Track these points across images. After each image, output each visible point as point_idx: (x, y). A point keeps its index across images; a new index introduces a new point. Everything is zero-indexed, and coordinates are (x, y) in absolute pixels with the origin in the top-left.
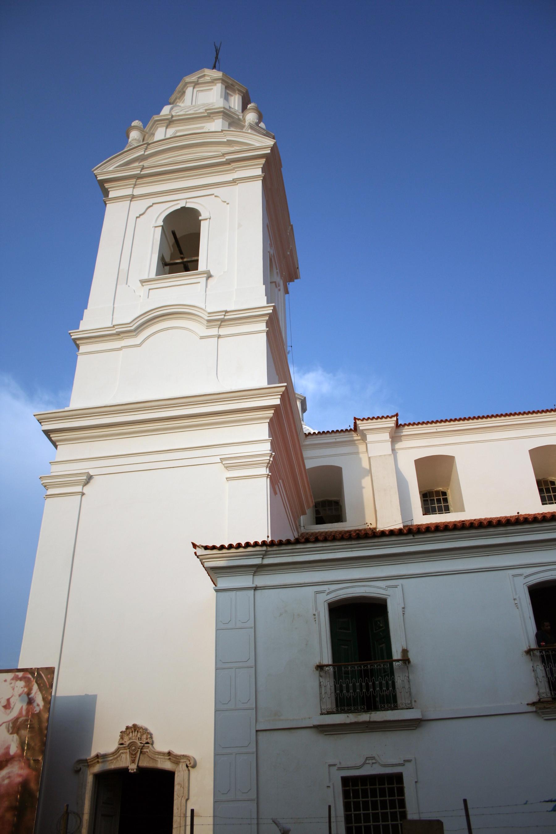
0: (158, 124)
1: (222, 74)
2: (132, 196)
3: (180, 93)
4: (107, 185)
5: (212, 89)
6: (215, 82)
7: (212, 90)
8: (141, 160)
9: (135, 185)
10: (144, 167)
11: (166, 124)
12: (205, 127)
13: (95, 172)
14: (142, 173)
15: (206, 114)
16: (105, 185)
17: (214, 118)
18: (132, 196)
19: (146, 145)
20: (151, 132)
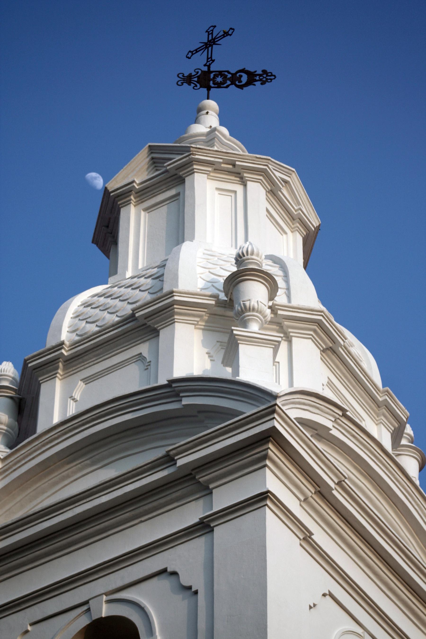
0: (315, 331)
1: (318, 224)
2: (308, 535)
3: (231, 166)
5: (286, 233)
6: (298, 225)
7: (285, 236)
8: (317, 434)
9: (306, 500)
10: (343, 483)
11: (324, 347)
12: (363, 422)
13: (278, 402)
14: (334, 492)
15: (380, 399)
16: (270, 446)
17: (383, 418)
18: (308, 535)
19: (341, 413)
20: (286, 323)
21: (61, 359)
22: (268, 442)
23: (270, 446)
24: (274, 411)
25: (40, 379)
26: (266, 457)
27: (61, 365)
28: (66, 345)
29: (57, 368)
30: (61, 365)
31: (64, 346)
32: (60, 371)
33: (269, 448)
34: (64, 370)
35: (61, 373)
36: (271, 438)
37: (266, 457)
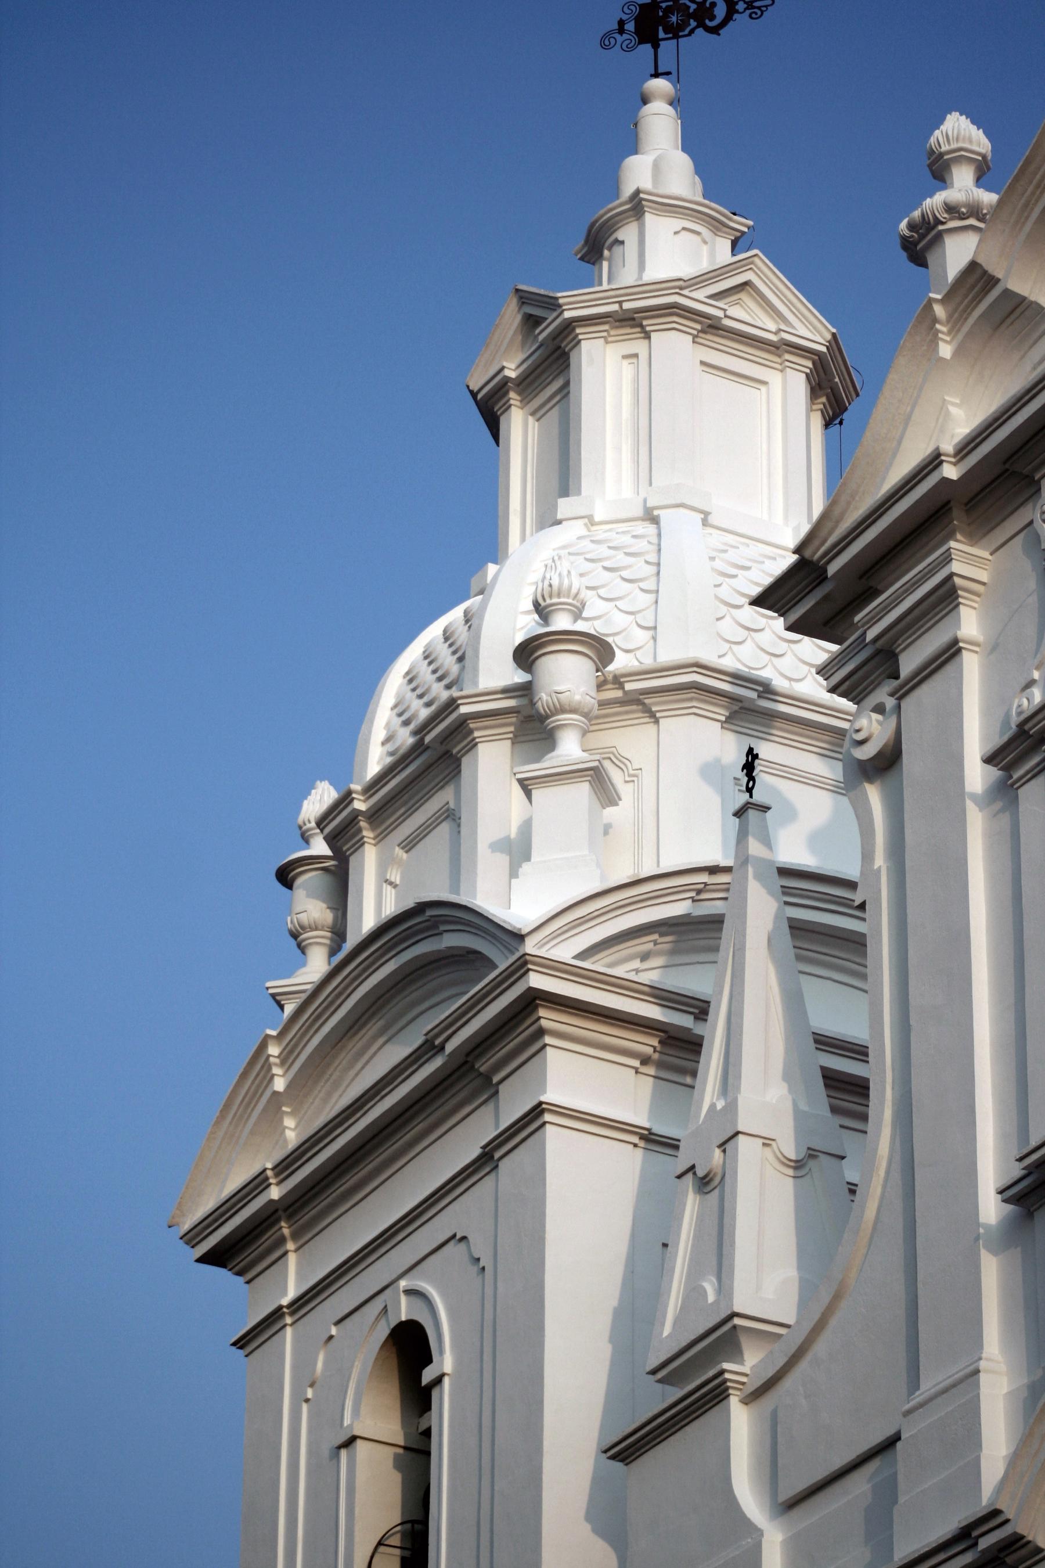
4: (548, 1018)
16: (542, 1012)
21: (360, 818)
22: (536, 1008)
23: (542, 1012)
24: (526, 963)
25: (344, 849)
26: (541, 1032)
27: (363, 824)
28: (356, 792)
29: (360, 830)
30: (363, 824)
31: (354, 795)
32: (365, 833)
33: (539, 1018)
34: (373, 829)
35: (371, 835)
36: (538, 1002)
37: (541, 1032)
